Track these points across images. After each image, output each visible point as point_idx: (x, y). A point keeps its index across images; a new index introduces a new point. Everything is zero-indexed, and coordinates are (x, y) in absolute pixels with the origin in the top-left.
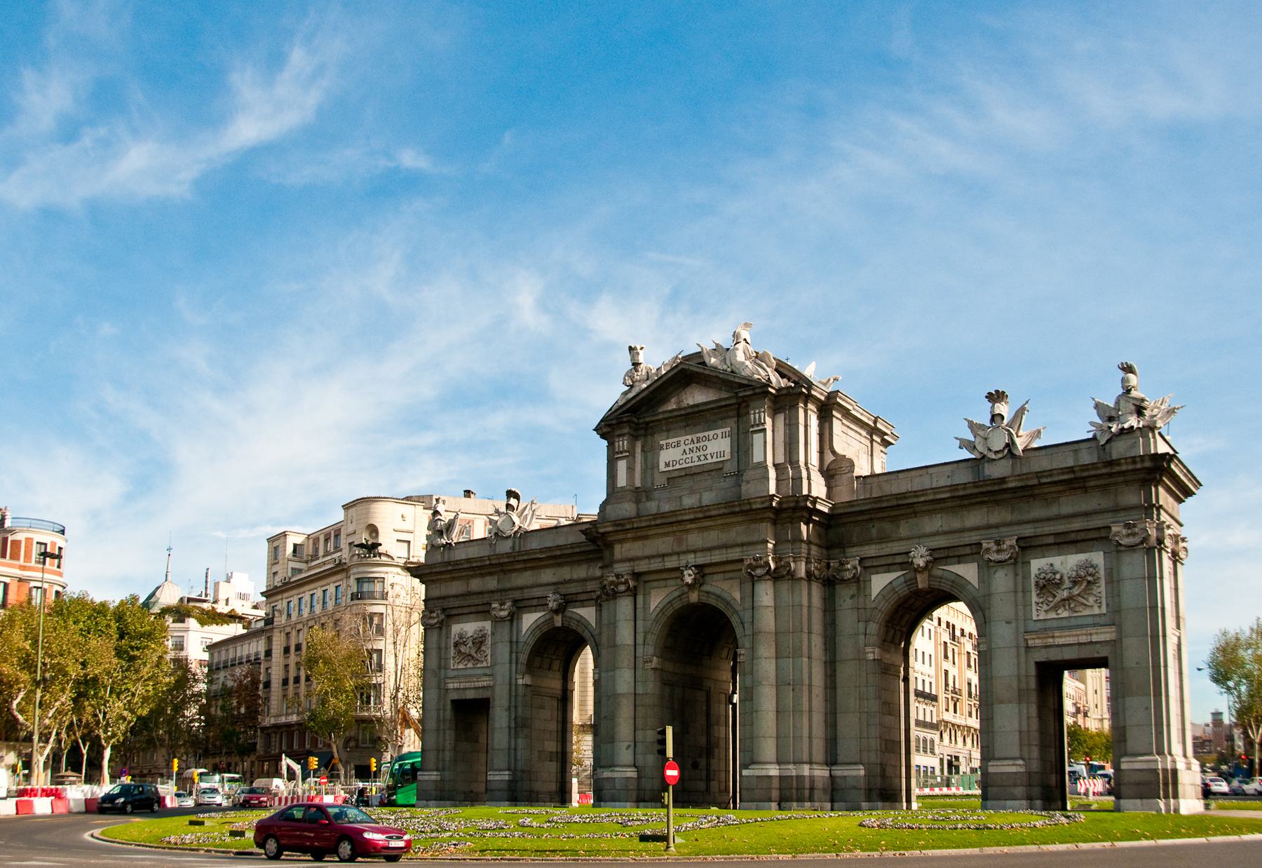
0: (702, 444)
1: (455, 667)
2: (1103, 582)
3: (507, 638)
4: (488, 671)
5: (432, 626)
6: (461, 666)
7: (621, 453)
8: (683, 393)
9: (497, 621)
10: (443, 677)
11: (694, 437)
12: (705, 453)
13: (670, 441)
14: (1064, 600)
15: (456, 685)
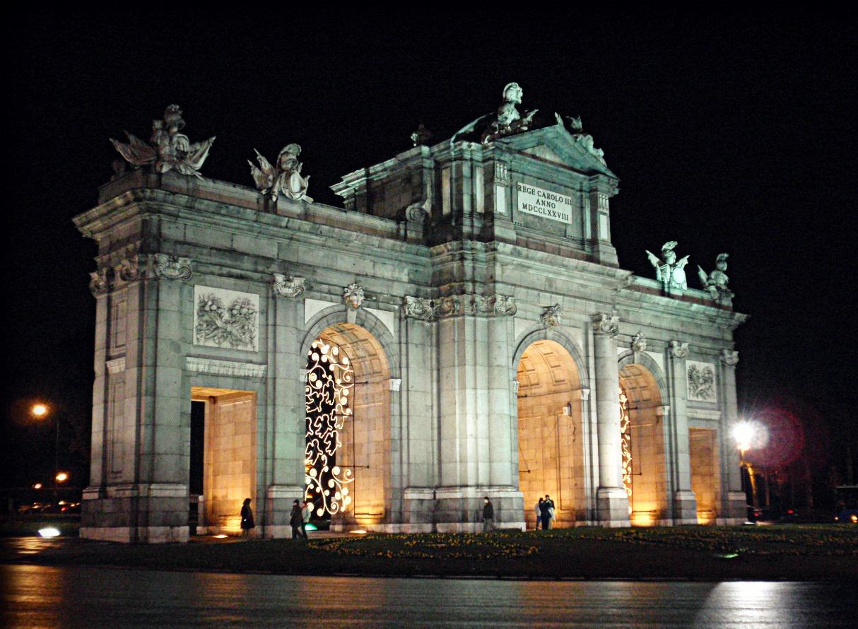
0: (551, 201)
1: (201, 343)
2: (714, 383)
3: (291, 323)
4: (254, 358)
5: (171, 279)
6: (211, 343)
7: (501, 179)
8: (537, 148)
9: (272, 299)
10: (184, 352)
11: (547, 192)
12: (555, 210)
13: (528, 186)
14: (702, 390)
15: (201, 368)
